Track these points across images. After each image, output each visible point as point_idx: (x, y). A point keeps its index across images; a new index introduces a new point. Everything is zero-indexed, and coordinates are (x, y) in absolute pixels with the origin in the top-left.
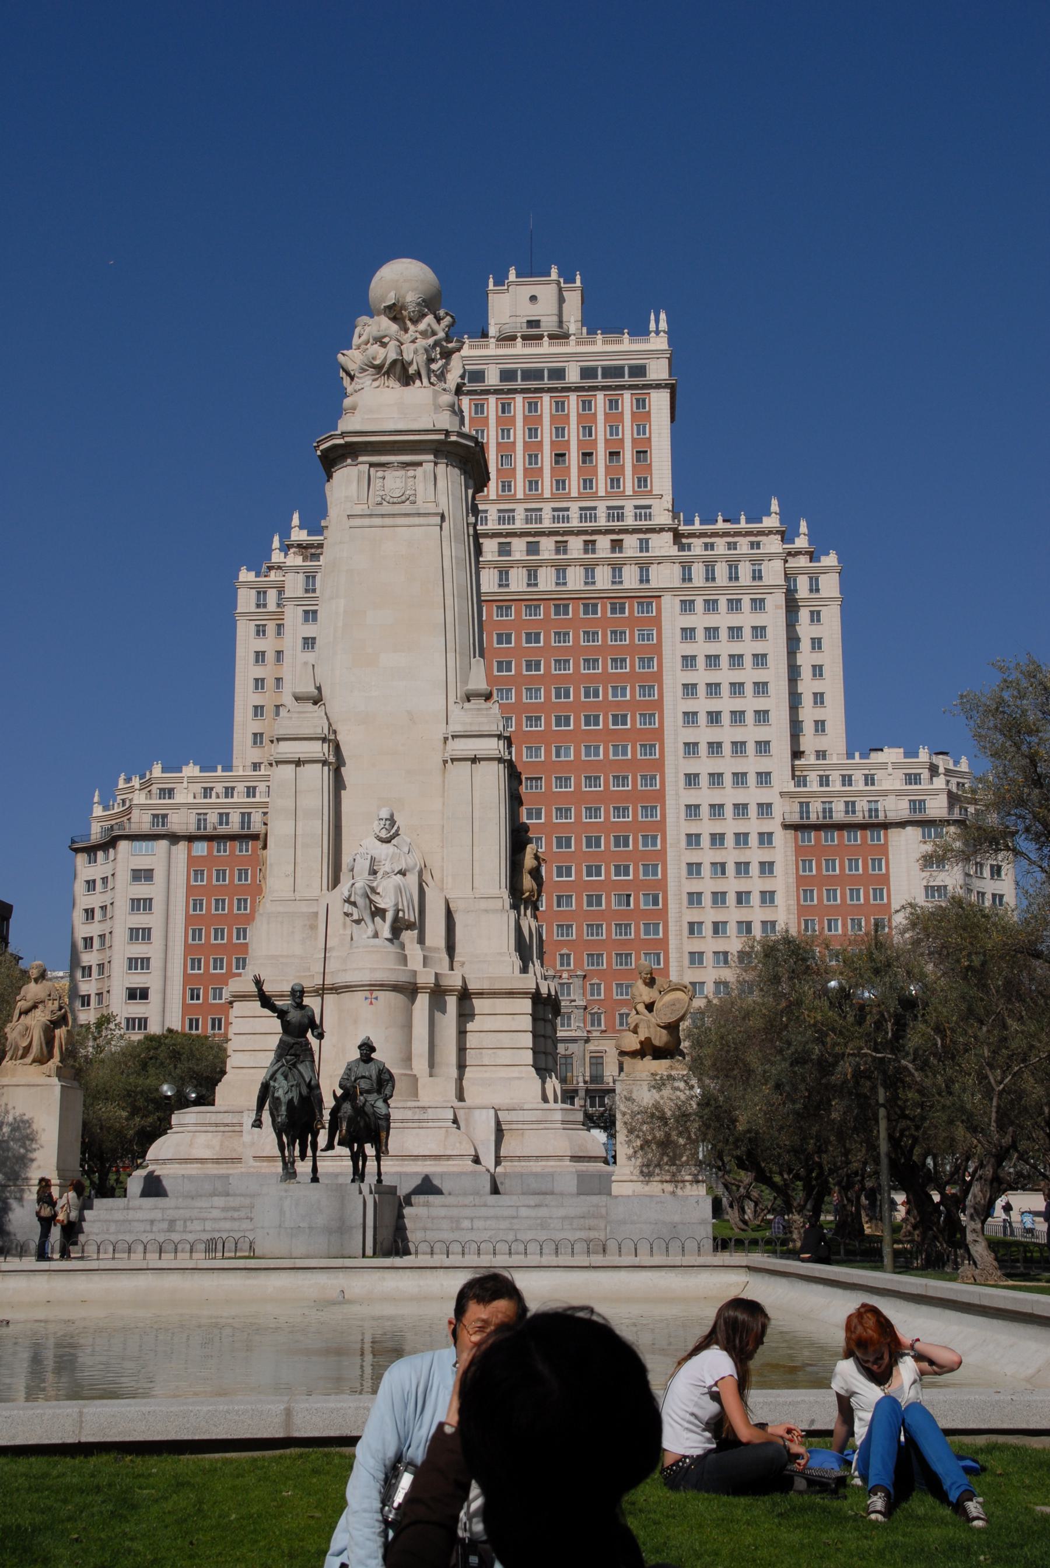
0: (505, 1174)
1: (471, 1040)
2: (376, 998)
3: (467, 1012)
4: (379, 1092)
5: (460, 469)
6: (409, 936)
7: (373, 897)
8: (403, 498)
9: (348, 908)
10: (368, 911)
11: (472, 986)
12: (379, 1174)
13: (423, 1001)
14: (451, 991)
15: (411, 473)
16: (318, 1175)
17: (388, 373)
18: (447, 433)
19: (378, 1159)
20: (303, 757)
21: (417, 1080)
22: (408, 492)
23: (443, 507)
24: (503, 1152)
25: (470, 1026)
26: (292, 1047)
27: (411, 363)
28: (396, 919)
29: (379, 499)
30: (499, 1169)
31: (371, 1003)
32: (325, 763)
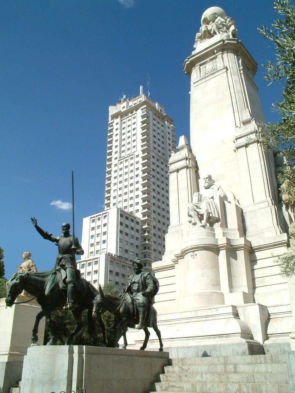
0: (271, 345)
1: (257, 274)
2: (196, 255)
3: (254, 259)
5: (234, 54)
6: (217, 226)
7: (198, 210)
8: (213, 70)
9: (190, 219)
10: (197, 217)
11: (254, 245)
13: (223, 254)
14: (240, 248)
15: (214, 61)
17: (205, 38)
18: (223, 41)
20: (178, 168)
21: (224, 295)
22: (215, 67)
23: (227, 64)
24: (269, 332)
25: (255, 267)
27: (211, 30)
28: (209, 218)
29: (204, 74)
30: (267, 342)
31: (194, 258)
32: (187, 167)
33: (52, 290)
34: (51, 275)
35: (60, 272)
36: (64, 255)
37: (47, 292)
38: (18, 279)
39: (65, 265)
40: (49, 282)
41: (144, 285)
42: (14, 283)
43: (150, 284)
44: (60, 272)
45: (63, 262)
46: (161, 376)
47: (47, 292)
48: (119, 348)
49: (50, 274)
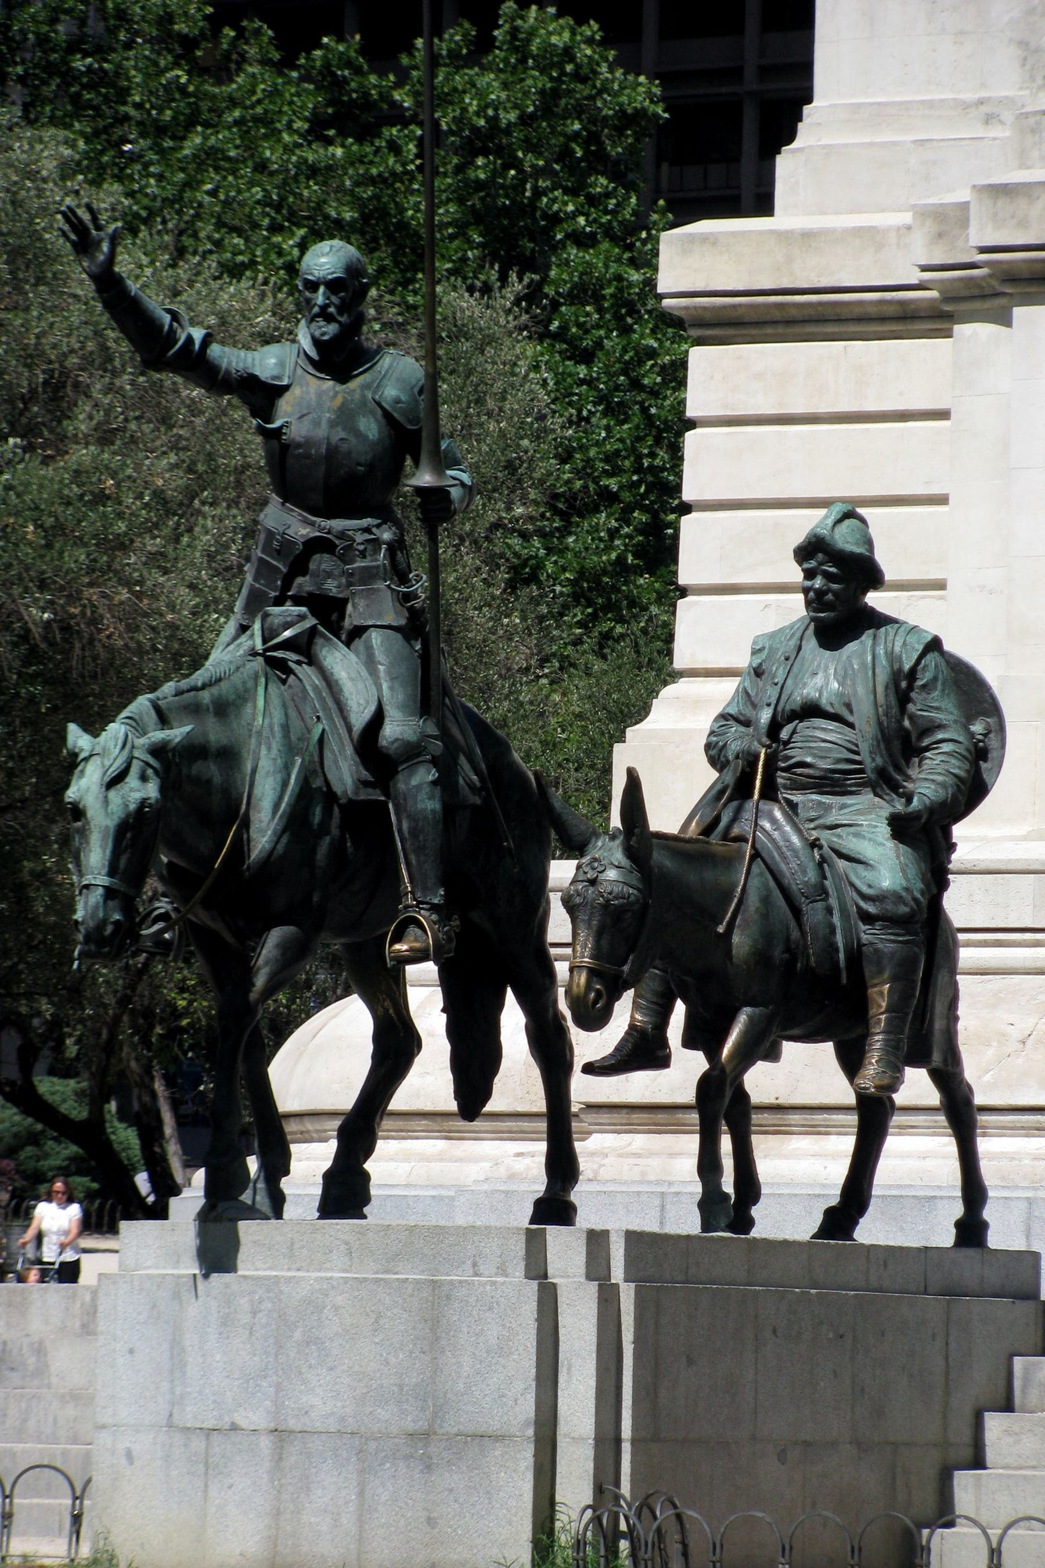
4: (887, 781)
12: (974, 1191)
16: (578, 1195)
19: (961, 1114)
26: (299, 565)
33: (296, 821)
34: (261, 690)
35: (312, 660)
36: (338, 524)
37: (264, 832)
38: (150, 772)
39: (344, 602)
40: (264, 751)
41: (902, 744)
42: (132, 807)
43: (940, 736)
44: (310, 663)
45: (326, 576)
46: (995, 1424)
47: (264, 832)
48: (755, 1233)
49: (256, 677)
